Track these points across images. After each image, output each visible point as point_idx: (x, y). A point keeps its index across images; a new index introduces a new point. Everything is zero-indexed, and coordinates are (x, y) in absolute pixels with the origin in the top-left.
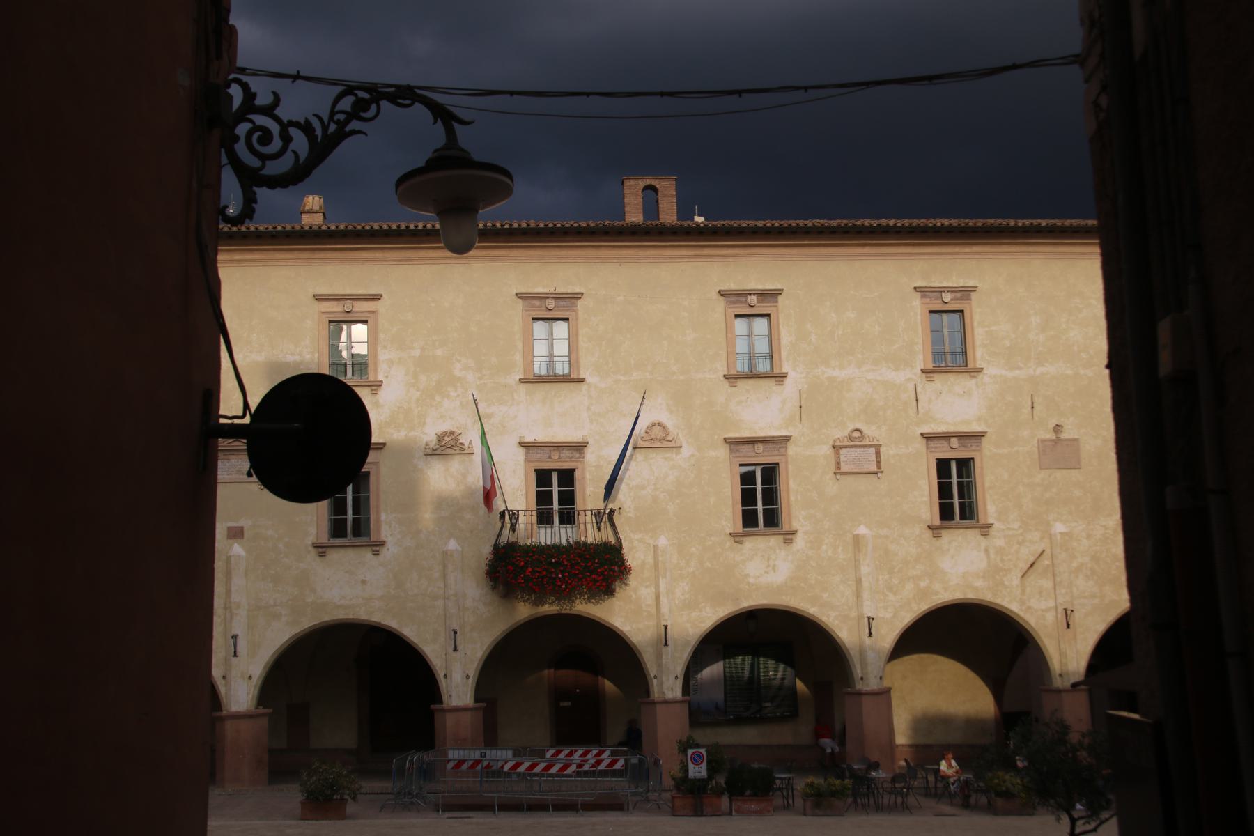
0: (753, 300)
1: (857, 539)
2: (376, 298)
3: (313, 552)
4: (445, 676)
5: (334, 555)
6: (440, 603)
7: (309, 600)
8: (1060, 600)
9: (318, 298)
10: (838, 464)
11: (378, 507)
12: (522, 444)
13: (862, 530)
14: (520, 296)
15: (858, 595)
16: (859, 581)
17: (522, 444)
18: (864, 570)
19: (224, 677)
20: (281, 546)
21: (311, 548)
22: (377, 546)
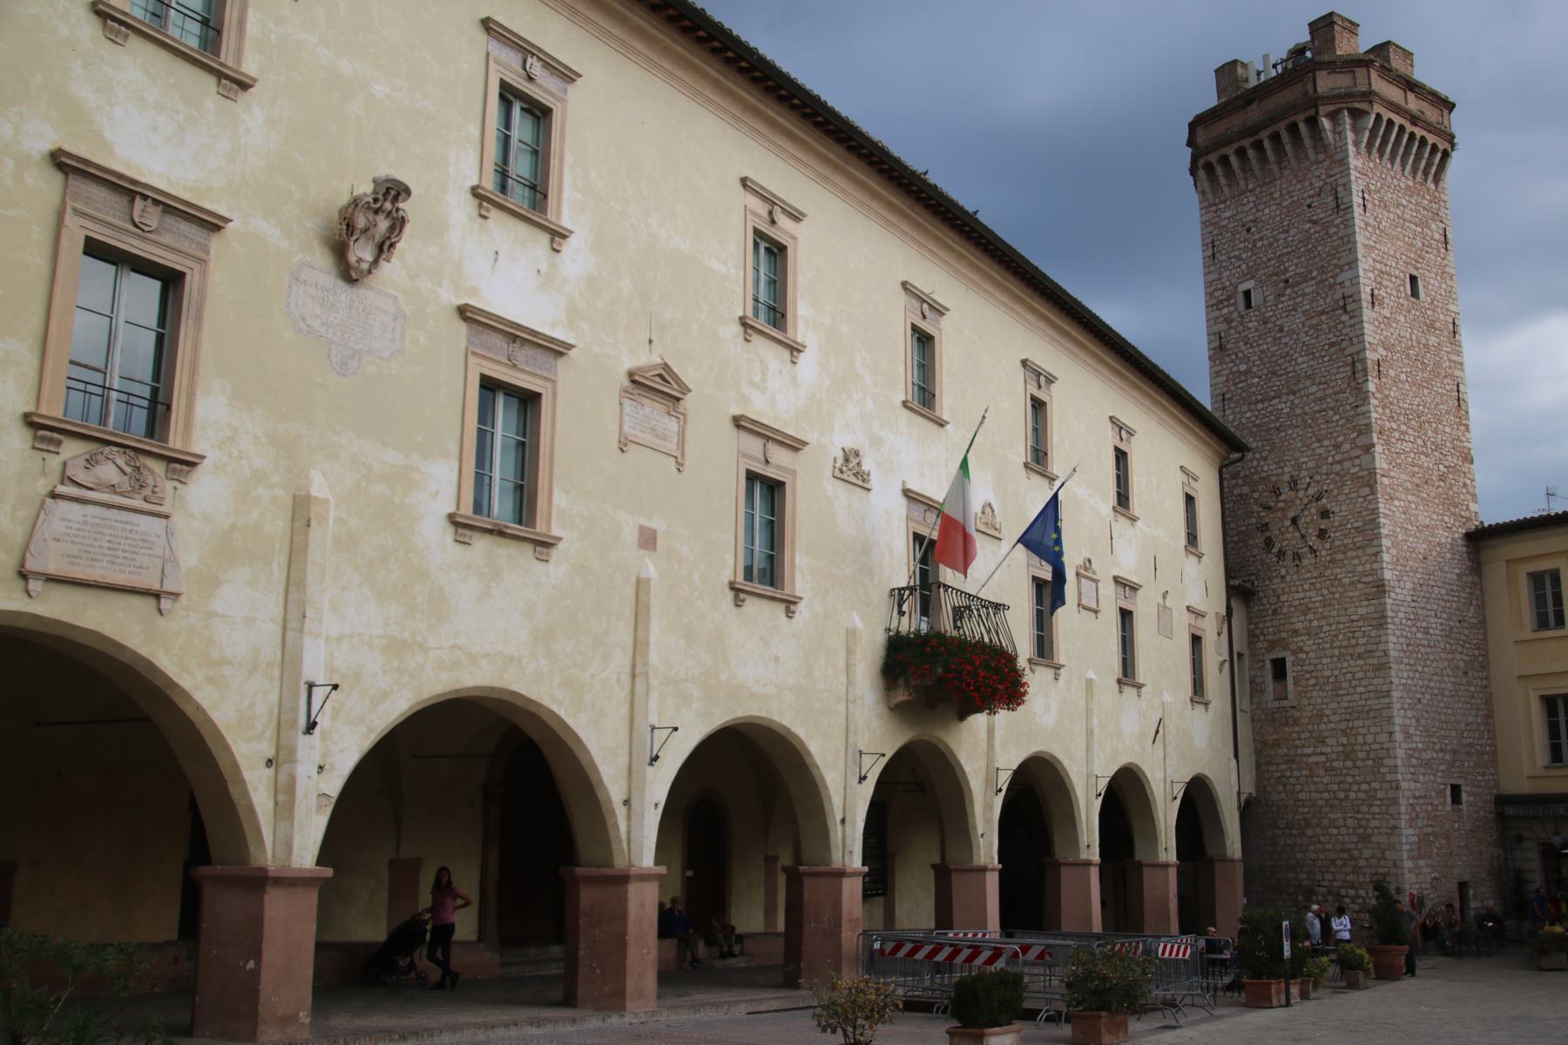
0: (1042, 379)
1: (1089, 683)
2: (796, 217)
3: (730, 595)
4: (843, 821)
5: (752, 606)
6: (842, 707)
7: (723, 678)
8: (1169, 771)
9: (744, 182)
10: (1080, 594)
11: (793, 542)
12: (908, 494)
13: (1091, 675)
14: (905, 285)
15: (1089, 749)
16: (1090, 733)
17: (908, 494)
18: (1095, 720)
19: (627, 802)
20: (696, 576)
21: (727, 590)
22: (790, 604)
